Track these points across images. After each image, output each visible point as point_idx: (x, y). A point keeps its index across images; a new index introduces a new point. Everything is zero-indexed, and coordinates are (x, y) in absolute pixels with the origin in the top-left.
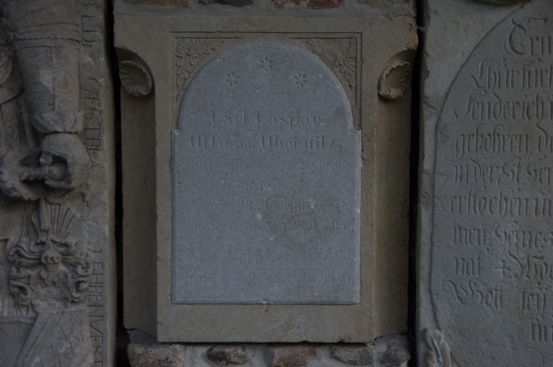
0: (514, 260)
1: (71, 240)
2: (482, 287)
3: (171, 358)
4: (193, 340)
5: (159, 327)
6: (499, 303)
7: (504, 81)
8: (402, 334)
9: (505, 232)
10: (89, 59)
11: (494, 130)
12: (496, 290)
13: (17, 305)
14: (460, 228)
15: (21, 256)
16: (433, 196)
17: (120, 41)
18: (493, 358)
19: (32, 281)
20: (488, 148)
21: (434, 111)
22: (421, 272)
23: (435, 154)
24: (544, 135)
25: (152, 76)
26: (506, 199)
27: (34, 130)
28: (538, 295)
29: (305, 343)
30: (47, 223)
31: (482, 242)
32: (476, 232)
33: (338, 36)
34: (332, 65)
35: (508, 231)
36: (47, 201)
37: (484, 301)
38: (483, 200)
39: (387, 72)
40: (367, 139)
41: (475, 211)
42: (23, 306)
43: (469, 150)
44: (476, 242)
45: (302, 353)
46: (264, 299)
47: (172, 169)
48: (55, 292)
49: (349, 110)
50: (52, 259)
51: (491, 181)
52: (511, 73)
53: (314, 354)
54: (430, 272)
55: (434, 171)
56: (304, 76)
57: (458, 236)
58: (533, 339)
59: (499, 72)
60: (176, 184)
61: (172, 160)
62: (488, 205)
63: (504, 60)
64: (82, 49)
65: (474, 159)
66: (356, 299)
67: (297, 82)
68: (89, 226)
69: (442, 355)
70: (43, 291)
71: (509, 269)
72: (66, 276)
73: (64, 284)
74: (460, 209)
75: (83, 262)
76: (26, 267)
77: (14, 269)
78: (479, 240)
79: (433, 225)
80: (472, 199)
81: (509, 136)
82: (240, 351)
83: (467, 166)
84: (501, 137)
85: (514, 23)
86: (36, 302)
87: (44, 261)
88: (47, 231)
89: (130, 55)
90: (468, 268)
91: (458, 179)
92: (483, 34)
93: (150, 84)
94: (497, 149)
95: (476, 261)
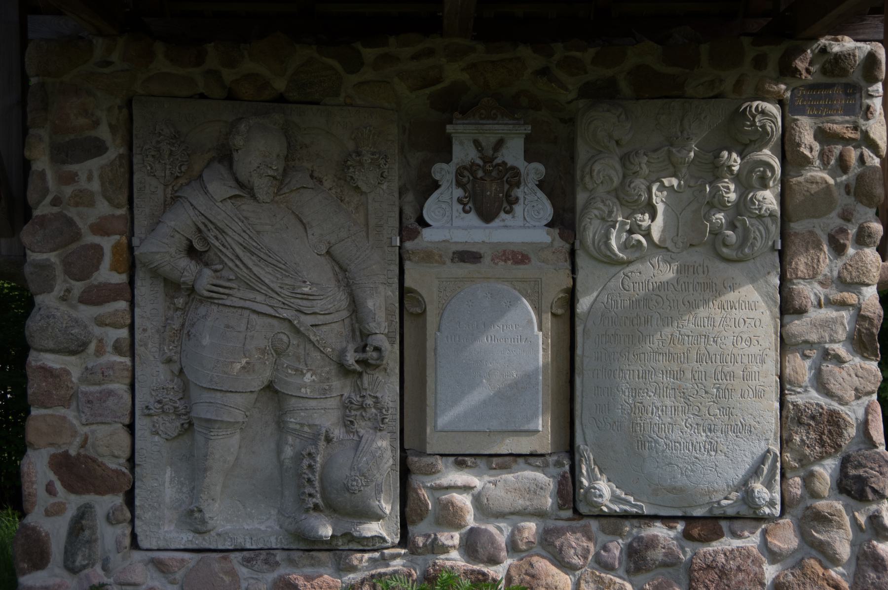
0: (627, 404)
1: (379, 395)
2: (610, 420)
3: (434, 463)
4: (447, 453)
5: (427, 445)
8: (566, 452)
10: (390, 293)
13: (348, 432)
15: (352, 403)
16: (583, 369)
17: (408, 283)
18: (617, 461)
19: (357, 418)
20: (612, 341)
23: (583, 345)
24: (641, 335)
25: (425, 302)
26: (622, 371)
27: (361, 332)
28: (640, 424)
30: (366, 385)
31: (610, 394)
36: (366, 372)
39: (556, 300)
40: (545, 336)
42: (352, 432)
44: (606, 395)
46: (488, 429)
47: (435, 354)
48: (369, 424)
50: (369, 405)
53: (516, 461)
54: (582, 413)
56: (510, 302)
57: (596, 392)
58: (638, 449)
60: (438, 362)
61: (435, 349)
63: (619, 294)
64: (387, 288)
68: (389, 387)
70: (363, 424)
72: (376, 415)
73: (375, 419)
75: (386, 407)
76: (354, 410)
77: (347, 411)
80: (604, 370)
82: (473, 459)
85: (624, 274)
86: (359, 430)
87: (365, 406)
88: (366, 390)
89: (411, 291)
90: (602, 410)
93: (424, 306)
94: (616, 343)
95: (607, 406)
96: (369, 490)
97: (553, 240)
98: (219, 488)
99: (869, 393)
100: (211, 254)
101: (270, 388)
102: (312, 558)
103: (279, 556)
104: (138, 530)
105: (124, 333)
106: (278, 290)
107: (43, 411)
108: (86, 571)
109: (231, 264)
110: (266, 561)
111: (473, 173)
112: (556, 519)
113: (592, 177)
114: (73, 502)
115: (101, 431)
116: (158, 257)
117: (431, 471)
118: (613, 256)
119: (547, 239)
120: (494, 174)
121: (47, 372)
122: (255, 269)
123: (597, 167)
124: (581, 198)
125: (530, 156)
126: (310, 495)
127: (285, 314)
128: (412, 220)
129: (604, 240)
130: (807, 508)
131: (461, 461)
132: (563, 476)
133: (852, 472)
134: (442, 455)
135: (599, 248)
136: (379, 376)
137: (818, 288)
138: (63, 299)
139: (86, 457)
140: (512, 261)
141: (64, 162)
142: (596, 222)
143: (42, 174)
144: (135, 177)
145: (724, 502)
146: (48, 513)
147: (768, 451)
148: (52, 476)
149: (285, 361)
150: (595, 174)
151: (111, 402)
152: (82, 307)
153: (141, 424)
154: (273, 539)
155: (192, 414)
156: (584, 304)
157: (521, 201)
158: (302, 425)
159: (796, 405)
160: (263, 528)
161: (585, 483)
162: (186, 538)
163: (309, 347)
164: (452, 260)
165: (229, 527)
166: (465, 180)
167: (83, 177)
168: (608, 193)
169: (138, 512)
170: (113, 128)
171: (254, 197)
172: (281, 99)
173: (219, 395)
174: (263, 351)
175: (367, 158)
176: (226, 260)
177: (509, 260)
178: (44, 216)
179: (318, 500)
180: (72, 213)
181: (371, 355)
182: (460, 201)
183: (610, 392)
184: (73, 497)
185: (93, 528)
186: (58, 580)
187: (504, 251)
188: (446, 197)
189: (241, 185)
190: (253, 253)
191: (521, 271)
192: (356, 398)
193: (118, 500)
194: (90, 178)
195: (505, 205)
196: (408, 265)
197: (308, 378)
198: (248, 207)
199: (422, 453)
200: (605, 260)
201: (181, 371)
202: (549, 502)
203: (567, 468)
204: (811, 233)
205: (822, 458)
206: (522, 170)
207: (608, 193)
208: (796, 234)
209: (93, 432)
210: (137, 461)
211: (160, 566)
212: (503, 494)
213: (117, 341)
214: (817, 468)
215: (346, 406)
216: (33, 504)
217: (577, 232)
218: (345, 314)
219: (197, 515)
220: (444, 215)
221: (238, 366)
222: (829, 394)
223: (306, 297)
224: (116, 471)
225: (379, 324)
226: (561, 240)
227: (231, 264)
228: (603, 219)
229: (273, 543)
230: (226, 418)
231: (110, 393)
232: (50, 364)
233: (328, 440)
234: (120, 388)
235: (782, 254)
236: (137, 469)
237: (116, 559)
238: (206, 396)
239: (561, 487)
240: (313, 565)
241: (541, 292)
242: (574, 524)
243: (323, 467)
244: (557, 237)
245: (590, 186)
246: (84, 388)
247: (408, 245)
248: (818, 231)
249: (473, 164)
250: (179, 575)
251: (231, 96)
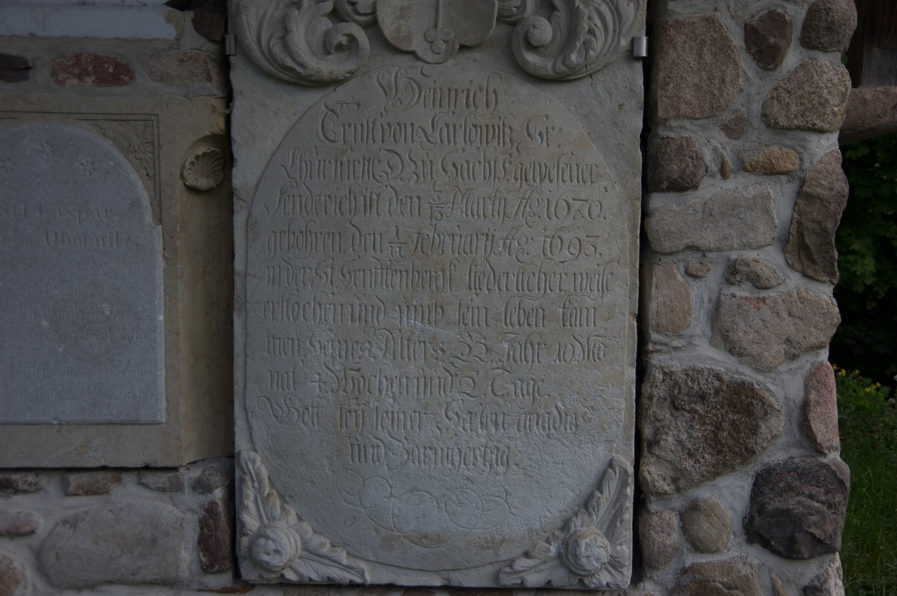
0: (330, 373)
2: (297, 402)
6: (315, 421)
7: (315, 172)
9: (319, 342)
11: (306, 227)
12: (313, 407)
14: (273, 338)
16: (246, 300)
18: (313, 483)
21: (245, 205)
22: (235, 387)
23: (247, 253)
24: (357, 233)
26: (320, 305)
28: (356, 411)
29: (104, 468)
31: (296, 352)
32: (290, 341)
33: (131, 117)
35: (322, 340)
37: (301, 419)
38: (296, 306)
39: (191, 158)
40: (169, 236)
41: (288, 316)
43: (281, 249)
44: (290, 353)
45: (103, 479)
46: (54, 419)
49: (146, 201)
51: (304, 284)
52: (322, 163)
53: (119, 480)
54: (245, 387)
55: (246, 274)
56: (93, 163)
57: (271, 346)
58: (353, 460)
59: (310, 161)
62: (301, 312)
63: (316, 148)
65: (286, 259)
66: (162, 417)
67: (85, 170)
69: (258, 480)
71: (325, 383)
74: (273, 316)
78: (293, 350)
79: (246, 335)
80: (285, 304)
81: (321, 233)
82: (31, 478)
83: (279, 267)
84: (314, 235)
85: (326, 107)
91: (271, 281)
92: (295, 119)
94: (309, 249)
95: (291, 375)
99: (815, 348)
112: (199, 590)
118: (299, 69)
119: (168, 32)
129: (278, 34)
130: (685, 571)
132: (211, 510)
133: (774, 504)
135: (270, 52)
137: (719, 138)
140: (93, 78)
145: (522, 563)
147: (611, 464)
159: (668, 374)
177: (89, 75)
183: (296, 348)
187: (78, 56)
200: (286, 77)
203: (218, 494)
204: (710, 22)
205: (717, 474)
208: (678, 24)
214: (704, 493)
217: (229, 19)
222: (732, 349)
226: (196, 34)
235: (649, 66)
239: (206, 531)
241: (159, 142)
244: (189, 27)
248: (724, 19)
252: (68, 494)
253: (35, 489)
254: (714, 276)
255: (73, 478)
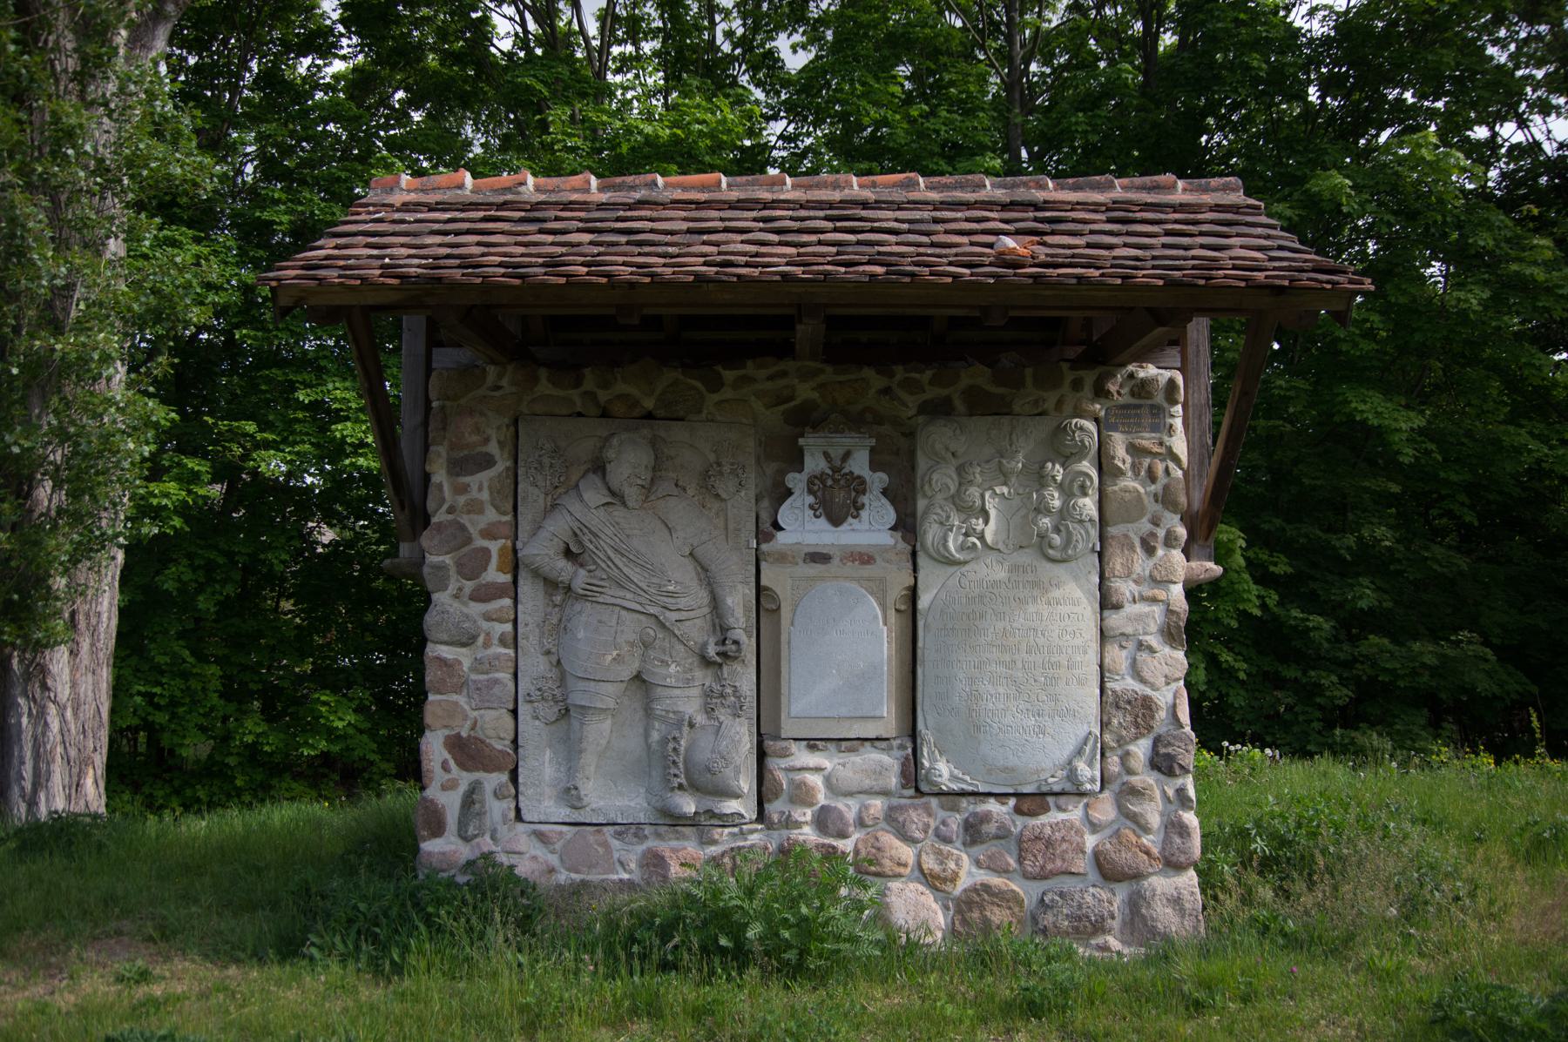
1: (737, 684)
13: (709, 718)
17: (764, 582)
27: (721, 626)
30: (726, 676)
34: (871, 594)
48: (729, 711)
61: (789, 643)
89: (767, 589)
96: (729, 772)
97: (896, 543)
98: (592, 769)
99: (1178, 680)
100: (586, 556)
101: (638, 678)
102: (677, 832)
103: (648, 830)
104: (521, 805)
105: (508, 627)
106: (645, 588)
107: (439, 697)
108: (477, 840)
109: (603, 565)
110: (636, 835)
111: (823, 482)
113: (931, 485)
114: (465, 779)
115: (489, 715)
116: (538, 558)
117: (785, 754)
119: (891, 542)
120: (842, 482)
121: (442, 662)
122: (625, 570)
123: (935, 477)
124: (921, 504)
125: (874, 466)
126: (675, 775)
127: (652, 610)
128: (768, 525)
130: (1124, 784)
131: (812, 744)
132: (907, 758)
133: (1163, 751)
134: (795, 739)
136: (737, 667)
137: (1132, 586)
138: (456, 597)
139: (476, 738)
141: (458, 475)
142: (935, 526)
143: (440, 486)
144: (520, 486)
145: (1051, 780)
146: (444, 788)
147: (1090, 733)
148: (448, 756)
149: (652, 653)
150: (933, 482)
151: (496, 690)
152: (472, 604)
153: (523, 709)
154: (642, 815)
155: (569, 701)
156: (924, 602)
157: (867, 507)
158: (667, 712)
159: (1114, 692)
160: (632, 804)
161: (926, 764)
162: (564, 813)
163: (674, 640)
164: (804, 561)
165: (602, 803)
166: (816, 488)
167: (475, 487)
168: (946, 499)
169: (521, 788)
170: (501, 444)
171: (624, 504)
172: (649, 416)
173: (592, 683)
174: (632, 644)
175: (727, 469)
176: (599, 561)
178: (441, 523)
179: (683, 780)
180: (465, 520)
181: (730, 647)
182: (811, 507)
184: (464, 774)
185: (482, 802)
186: (453, 847)
188: (798, 503)
189: (613, 493)
190: (623, 555)
191: (868, 571)
192: (716, 687)
193: (504, 777)
194: (480, 489)
195: (852, 510)
196: (763, 565)
197: (673, 668)
198: (619, 512)
199: (777, 737)
201: (559, 662)
202: (893, 781)
203: (910, 750)
204: (1126, 536)
205: (1137, 738)
206: (868, 479)
207: (946, 499)
208: (1113, 537)
209: (481, 717)
210: (520, 743)
211: (542, 837)
212: (851, 774)
213: (502, 634)
214: (1132, 748)
215: (708, 694)
216: (431, 779)
218: (706, 610)
219: (573, 792)
220: (797, 520)
221: (609, 658)
222: (1143, 681)
223: (671, 595)
224: (500, 751)
225: (737, 619)
227: (603, 565)
228: (941, 523)
229: (642, 818)
230: (599, 705)
231: (496, 681)
232: (445, 655)
233: (691, 725)
234: (505, 676)
235: (1101, 555)
236: (520, 750)
237: (503, 830)
238: (581, 685)
240: (678, 839)
242: (916, 801)
243: (687, 750)
245: (929, 493)
246: (474, 677)
247: (764, 547)
248: (1132, 535)
249: (823, 473)
250: (558, 846)
251: (605, 414)
252: (840, 751)
253: (825, 749)
254: (1131, 645)
255: (844, 744)
